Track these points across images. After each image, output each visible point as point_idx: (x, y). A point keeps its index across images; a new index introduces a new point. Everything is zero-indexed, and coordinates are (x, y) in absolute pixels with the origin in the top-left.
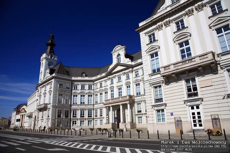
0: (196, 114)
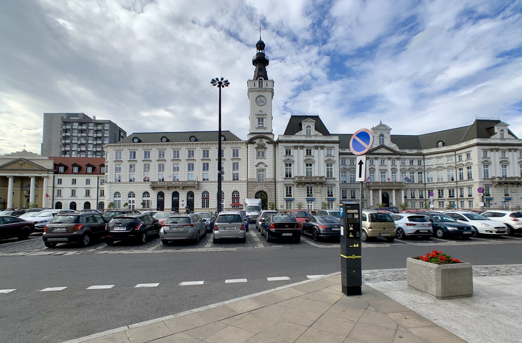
0: (310, 206)
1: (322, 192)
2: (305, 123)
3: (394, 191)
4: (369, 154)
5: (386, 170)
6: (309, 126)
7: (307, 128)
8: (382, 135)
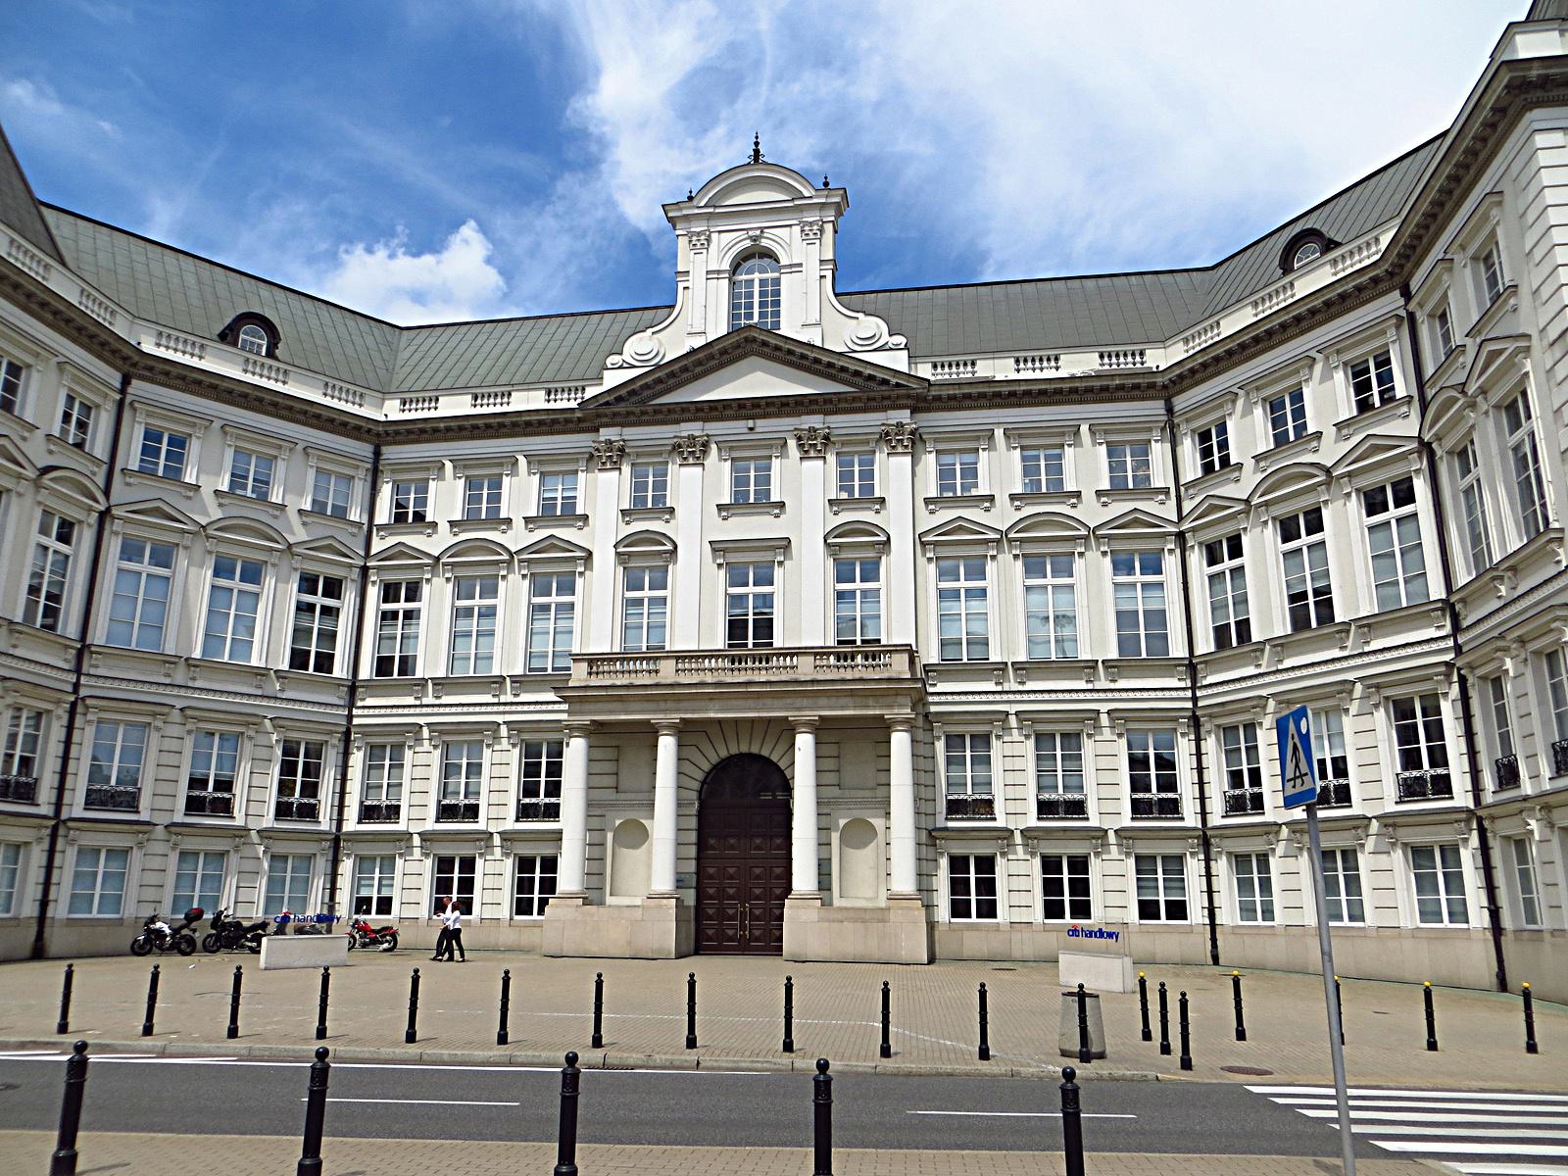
3: (804, 742)
4: (618, 421)
5: (785, 545)
8: (756, 254)
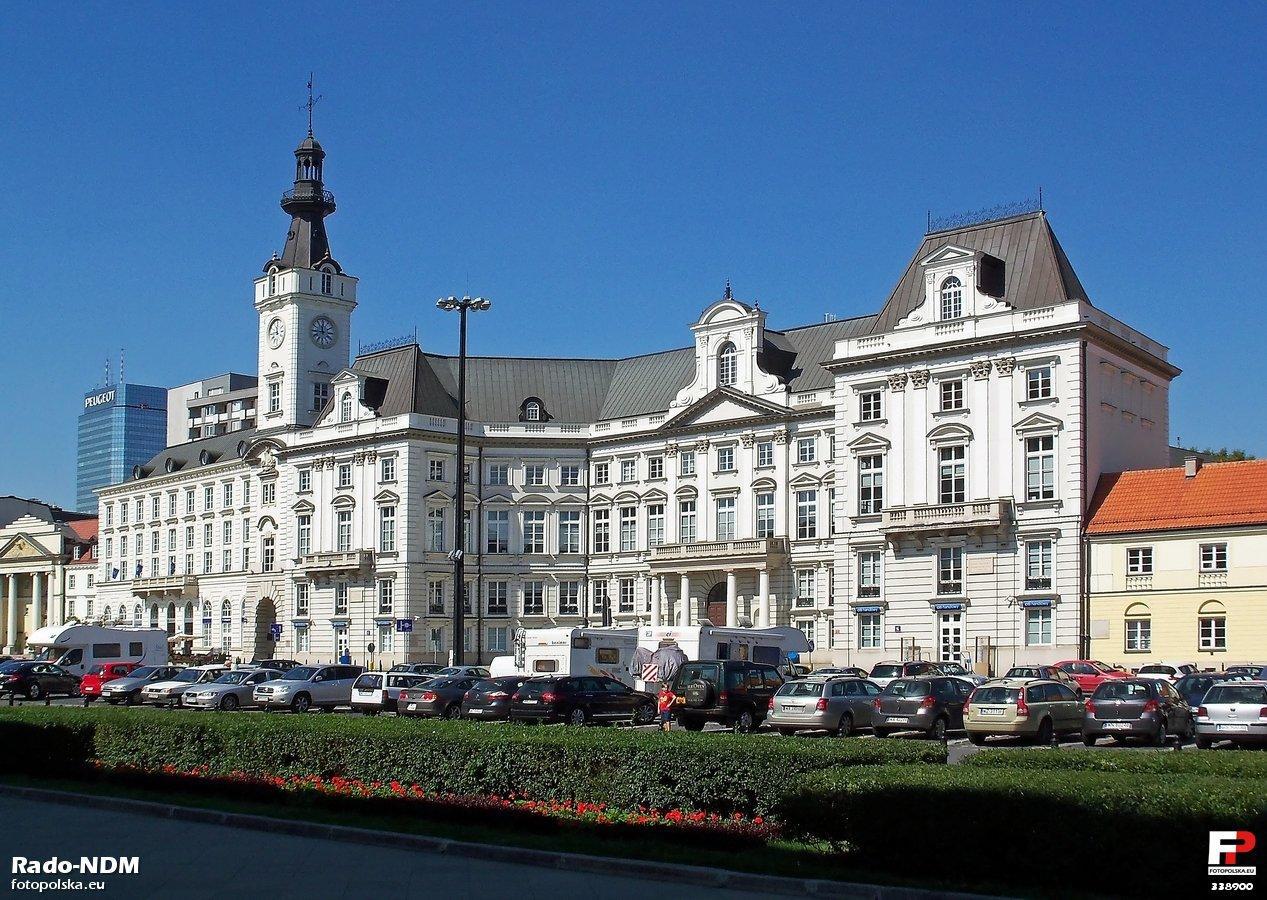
0: (951, 632)
1: (1000, 569)
2: (935, 270)
6: (951, 280)
7: (944, 286)
